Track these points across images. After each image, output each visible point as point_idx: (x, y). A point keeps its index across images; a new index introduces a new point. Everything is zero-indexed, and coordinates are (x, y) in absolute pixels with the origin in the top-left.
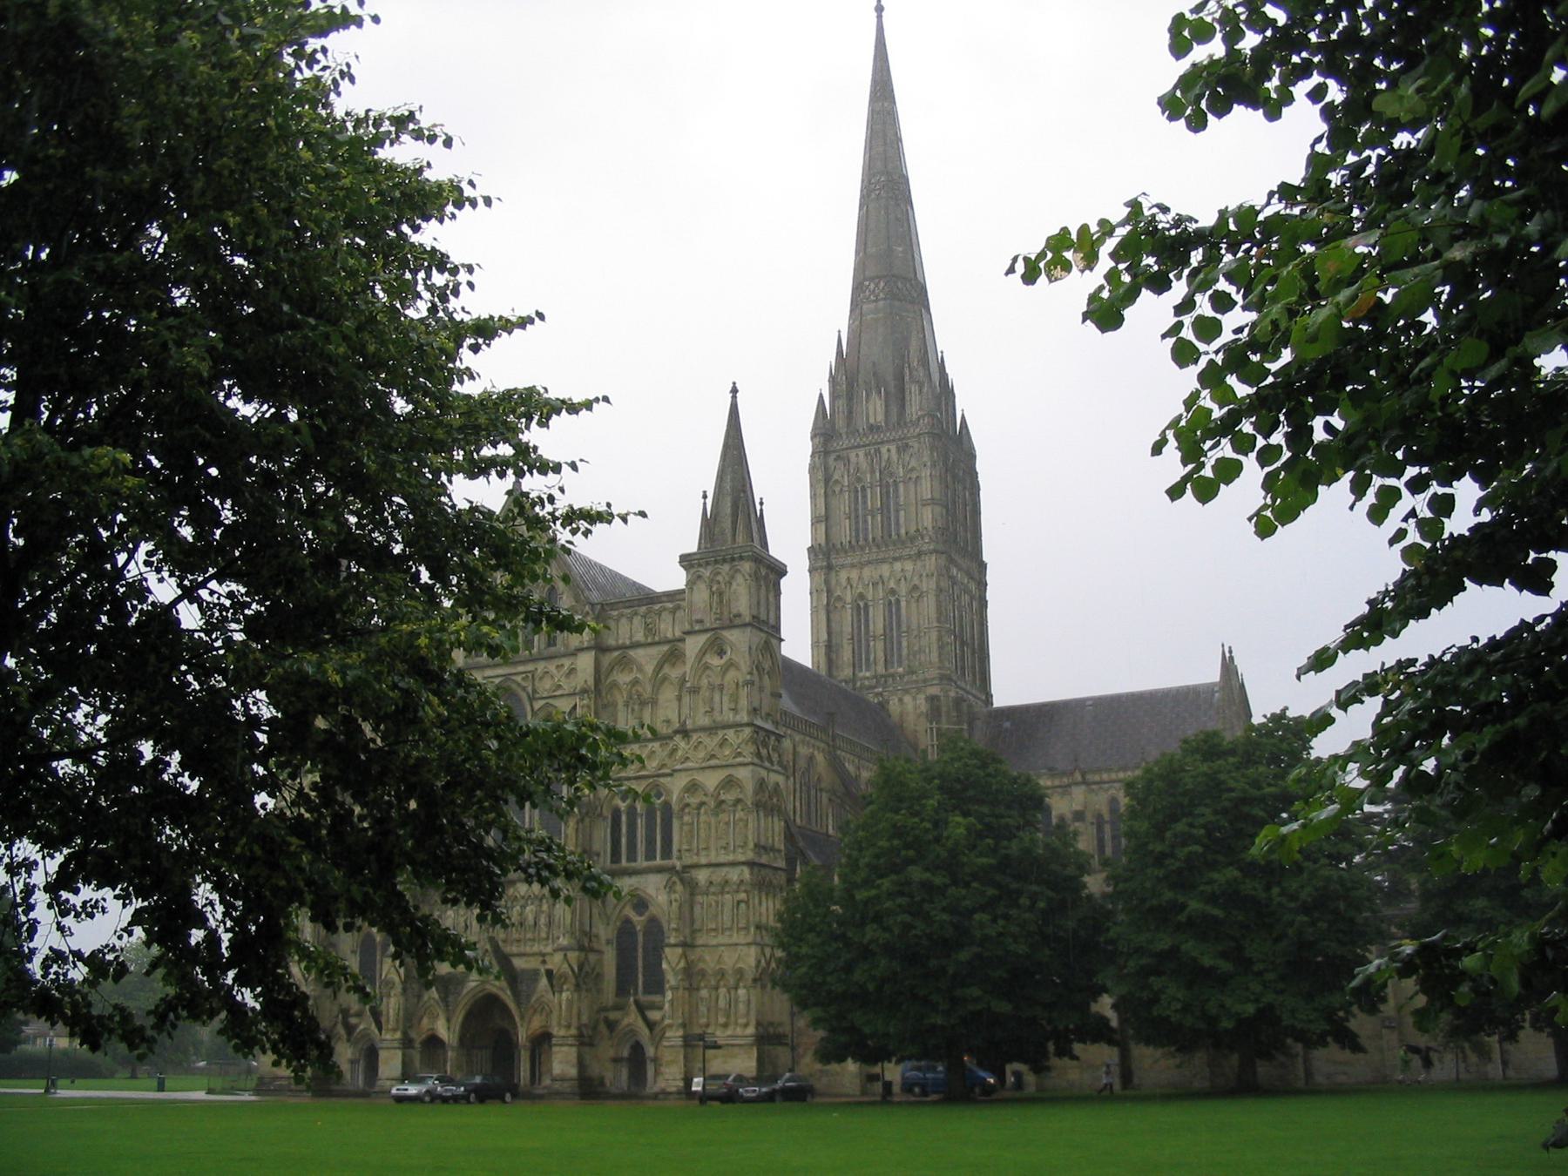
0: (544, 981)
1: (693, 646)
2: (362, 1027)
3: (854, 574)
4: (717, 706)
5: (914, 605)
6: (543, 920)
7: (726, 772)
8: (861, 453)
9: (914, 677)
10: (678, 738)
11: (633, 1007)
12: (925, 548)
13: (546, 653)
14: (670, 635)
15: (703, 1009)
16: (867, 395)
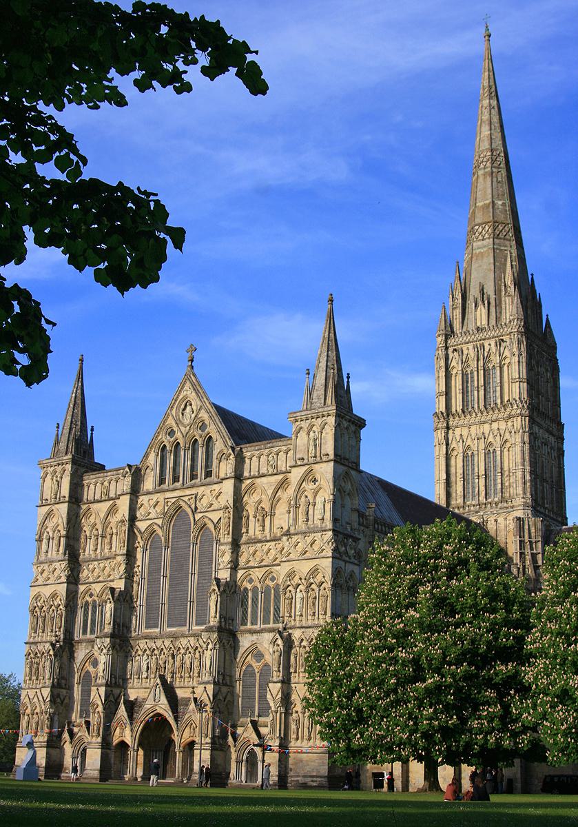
0: (192, 706)
1: (297, 474)
2: (79, 734)
3: (465, 432)
4: (311, 518)
5: (506, 453)
6: (196, 664)
7: (312, 564)
8: (471, 346)
9: (505, 505)
10: (285, 538)
11: (250, 725)
12: (513, 413)
13: (204, 481)
14: (284, 469)
15: (293, 727)
16: (476, 306)
